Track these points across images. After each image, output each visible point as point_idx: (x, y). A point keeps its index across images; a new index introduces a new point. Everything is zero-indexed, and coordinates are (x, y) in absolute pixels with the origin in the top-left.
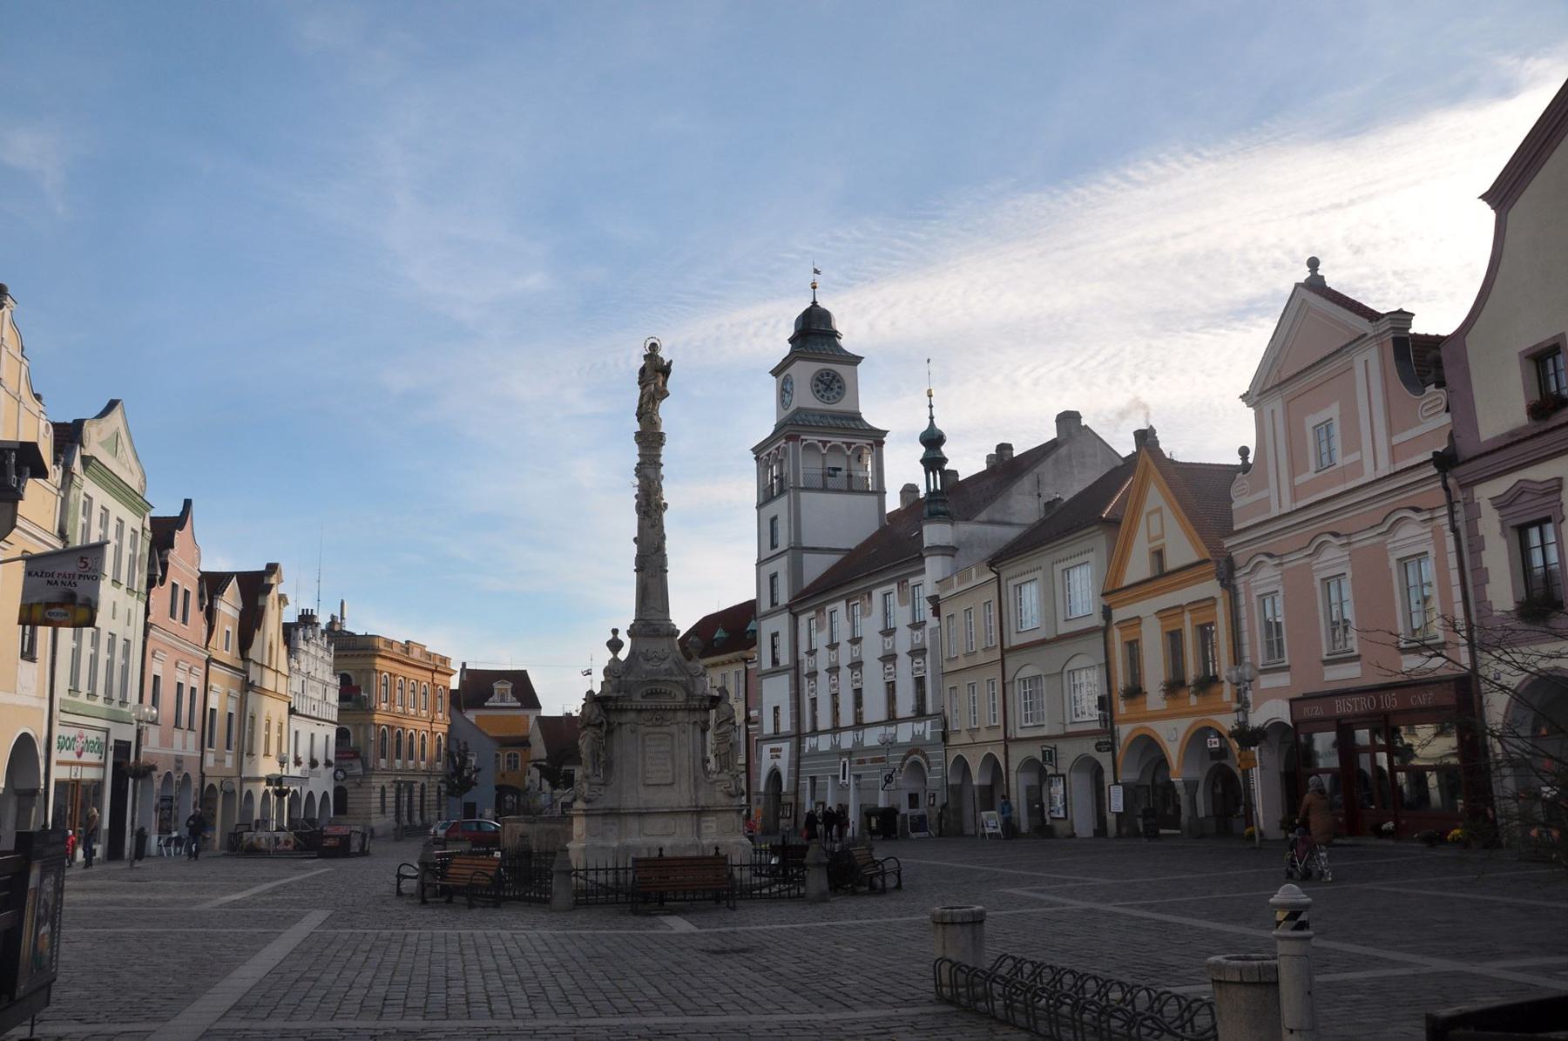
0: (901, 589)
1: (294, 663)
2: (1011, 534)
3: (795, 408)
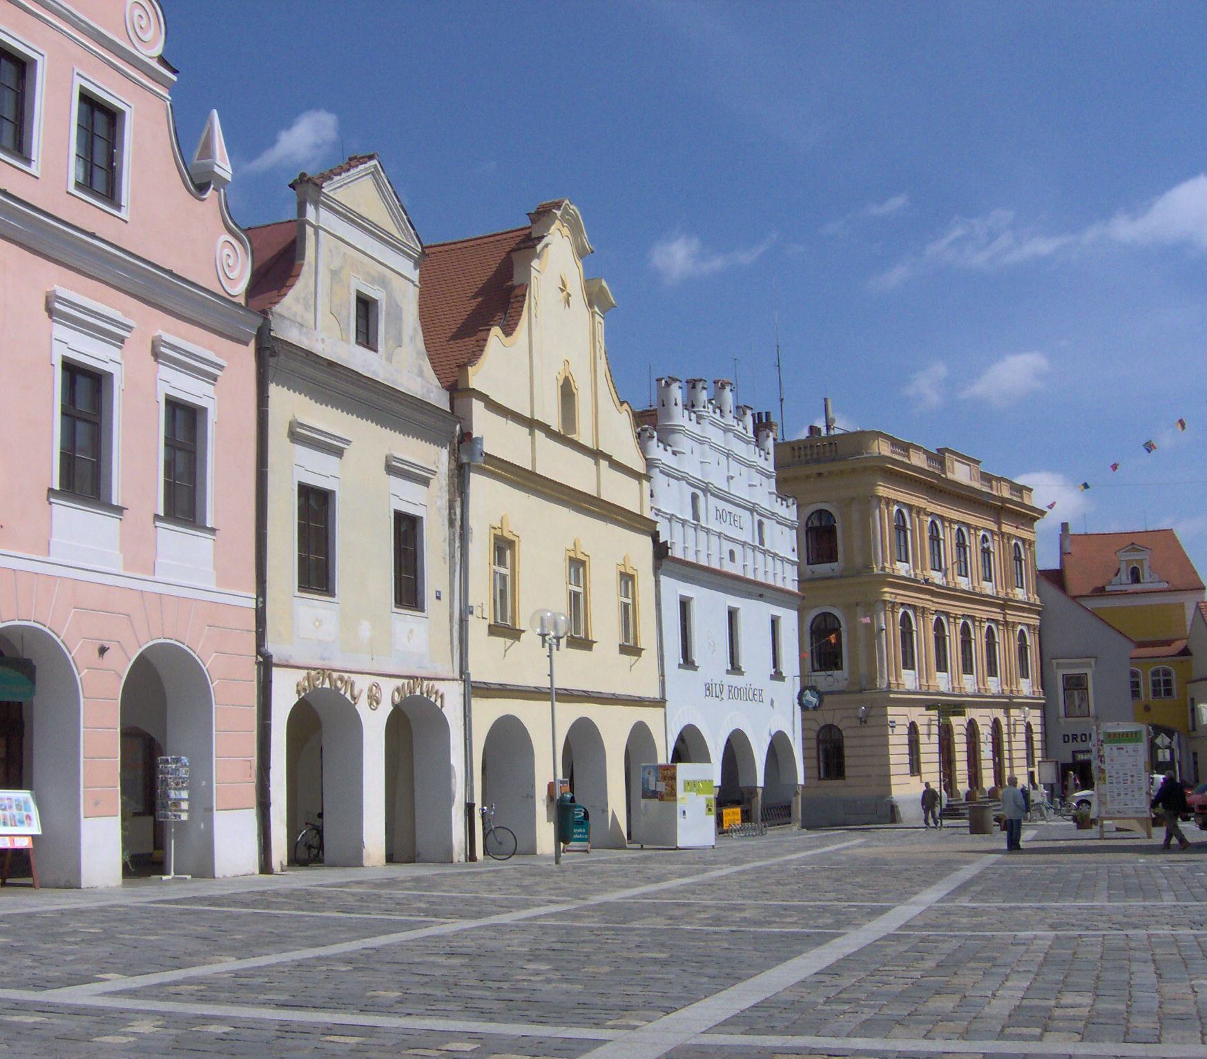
1: (656, 451)
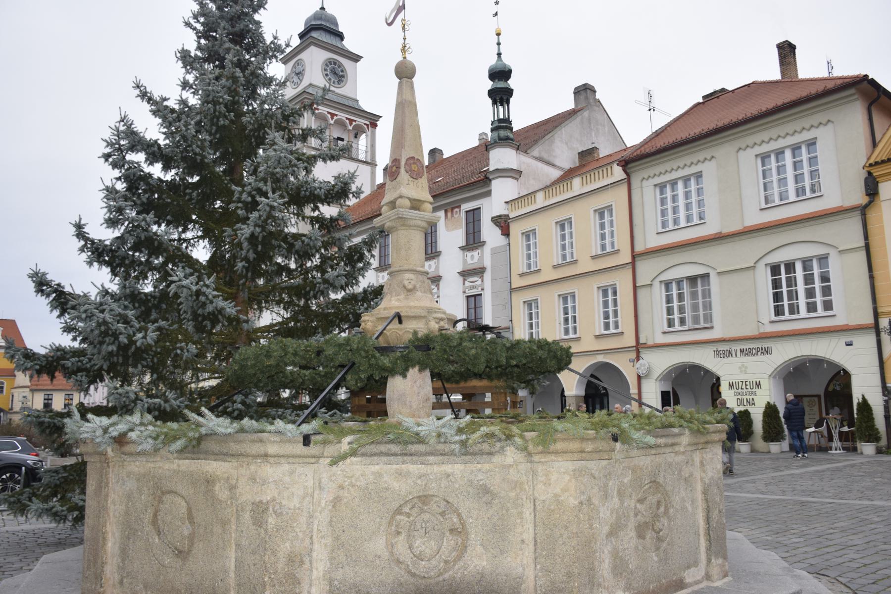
0: (449, 214)
2: (556, 174)
3: (307, 84)
